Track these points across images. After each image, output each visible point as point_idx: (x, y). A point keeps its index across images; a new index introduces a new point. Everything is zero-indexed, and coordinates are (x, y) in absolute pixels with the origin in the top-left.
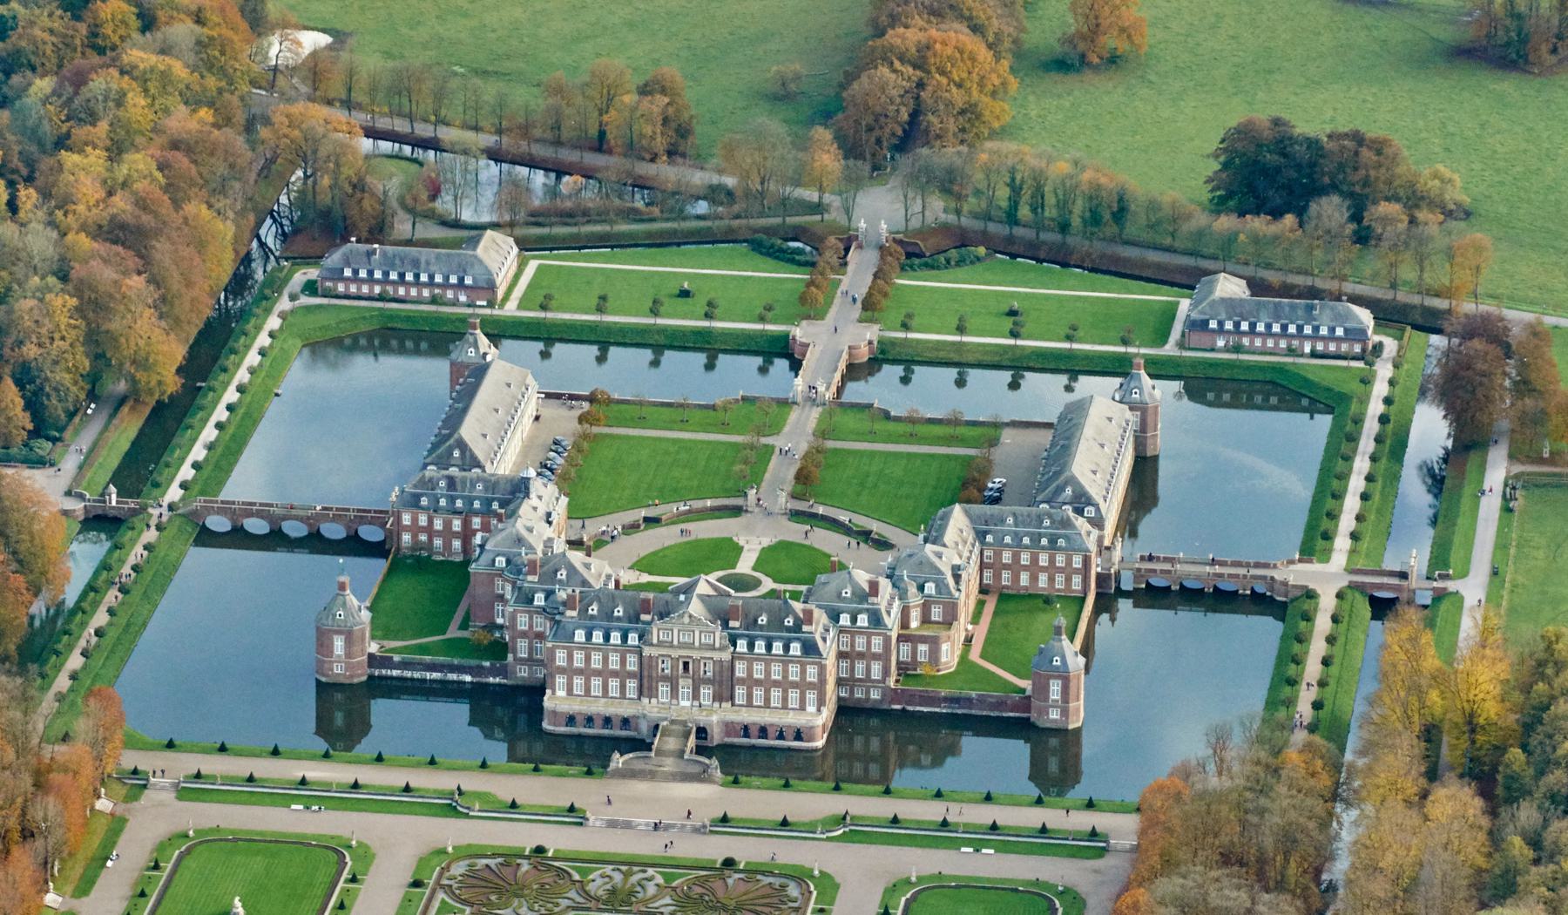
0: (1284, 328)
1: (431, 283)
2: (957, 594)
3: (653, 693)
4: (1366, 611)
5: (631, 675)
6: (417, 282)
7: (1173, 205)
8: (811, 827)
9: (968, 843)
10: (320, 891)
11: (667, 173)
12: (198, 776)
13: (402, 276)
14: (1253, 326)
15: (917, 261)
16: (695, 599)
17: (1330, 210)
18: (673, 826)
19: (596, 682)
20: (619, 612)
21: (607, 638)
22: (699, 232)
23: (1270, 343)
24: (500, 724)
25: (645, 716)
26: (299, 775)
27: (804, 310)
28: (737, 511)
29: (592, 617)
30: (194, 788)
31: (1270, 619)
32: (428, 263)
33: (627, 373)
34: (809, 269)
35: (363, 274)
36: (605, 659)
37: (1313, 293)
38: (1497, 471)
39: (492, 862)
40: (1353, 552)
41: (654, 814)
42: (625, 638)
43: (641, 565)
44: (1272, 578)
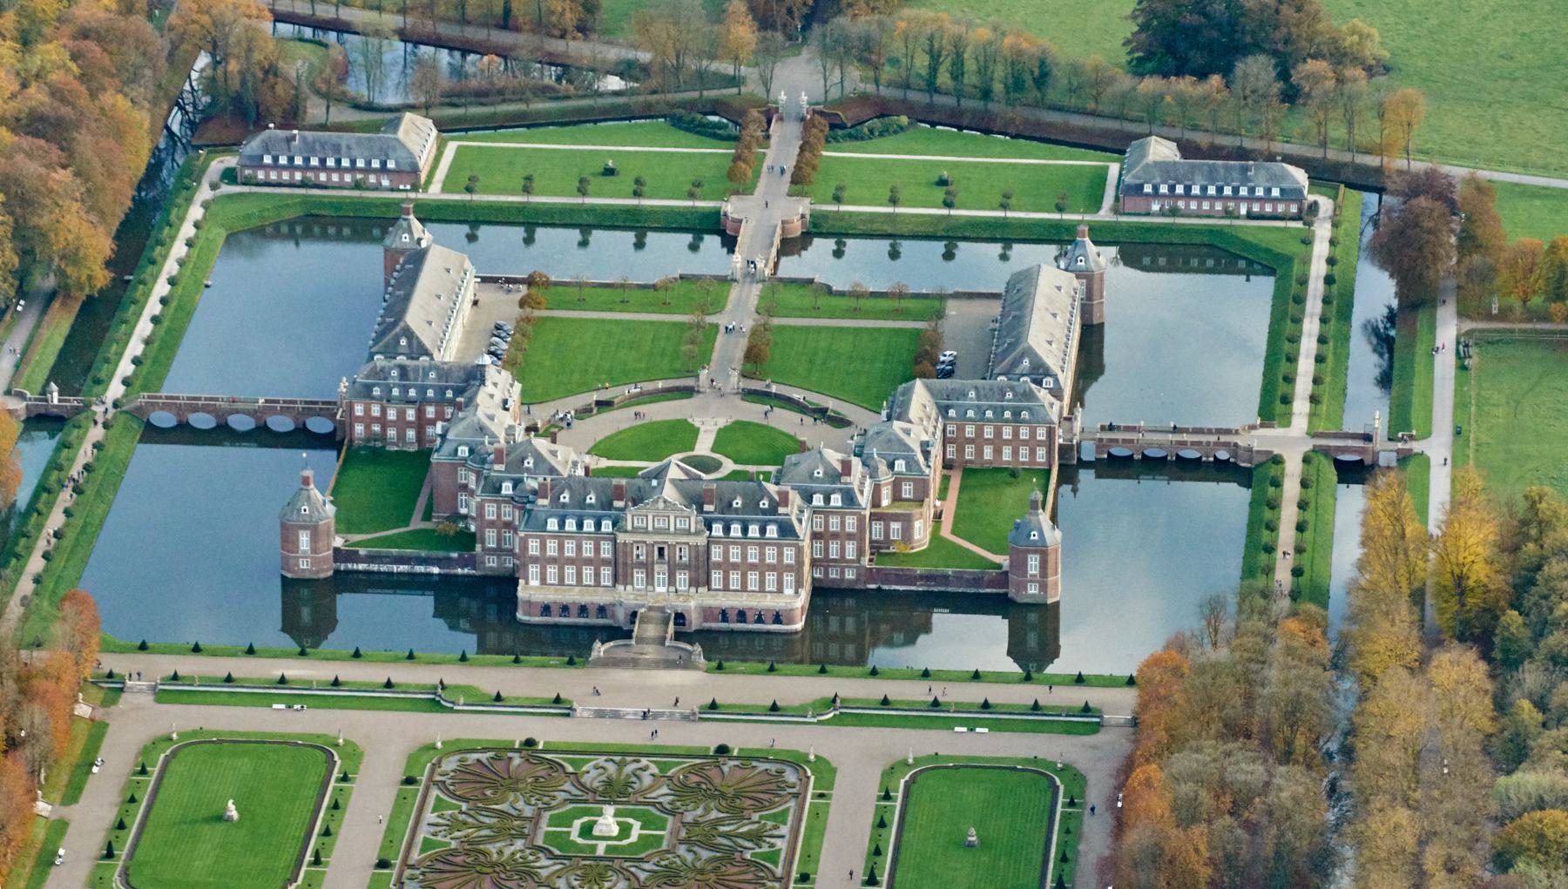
0: (1220, 190)
1: (353, 168)
2: (927, 471)
3: (628, 580)
4: (1331, 473)
5: (605, 562)
6: (338, 167)
7: (1096, 69)
8: (801, 711)
9: (962, 722)
10: (312, 792)
11: (578, 49)
12: (175, 677)
13: (323, 161)
14: (1188, 189)
15: (840, 132)
16: (668, 485)
17: (1257, 69)
18: (662, 714)
19: (570, 571)
20: (591, 499)
21: (580, 525)
22: (614, 108)
23: (1206, 206)
24: (466, 614)
25: (621, 604)
26: (277, 674)
27: (733, 186)
28: (688, 392)
29: (564, 505)
30: (172, 690)
31: (1234, 486)
32: (349, 147)
33: (557, 253)
34: (733, 143)
35: (283, 161)
36: (579, 548)
37: (1242, 154)
38: (1448, 329)
39: (484, 757)
40: (1312, 415)
41: (640, 703)
42: (598, 525)
43: (598, 450)
44: (1236, 445)
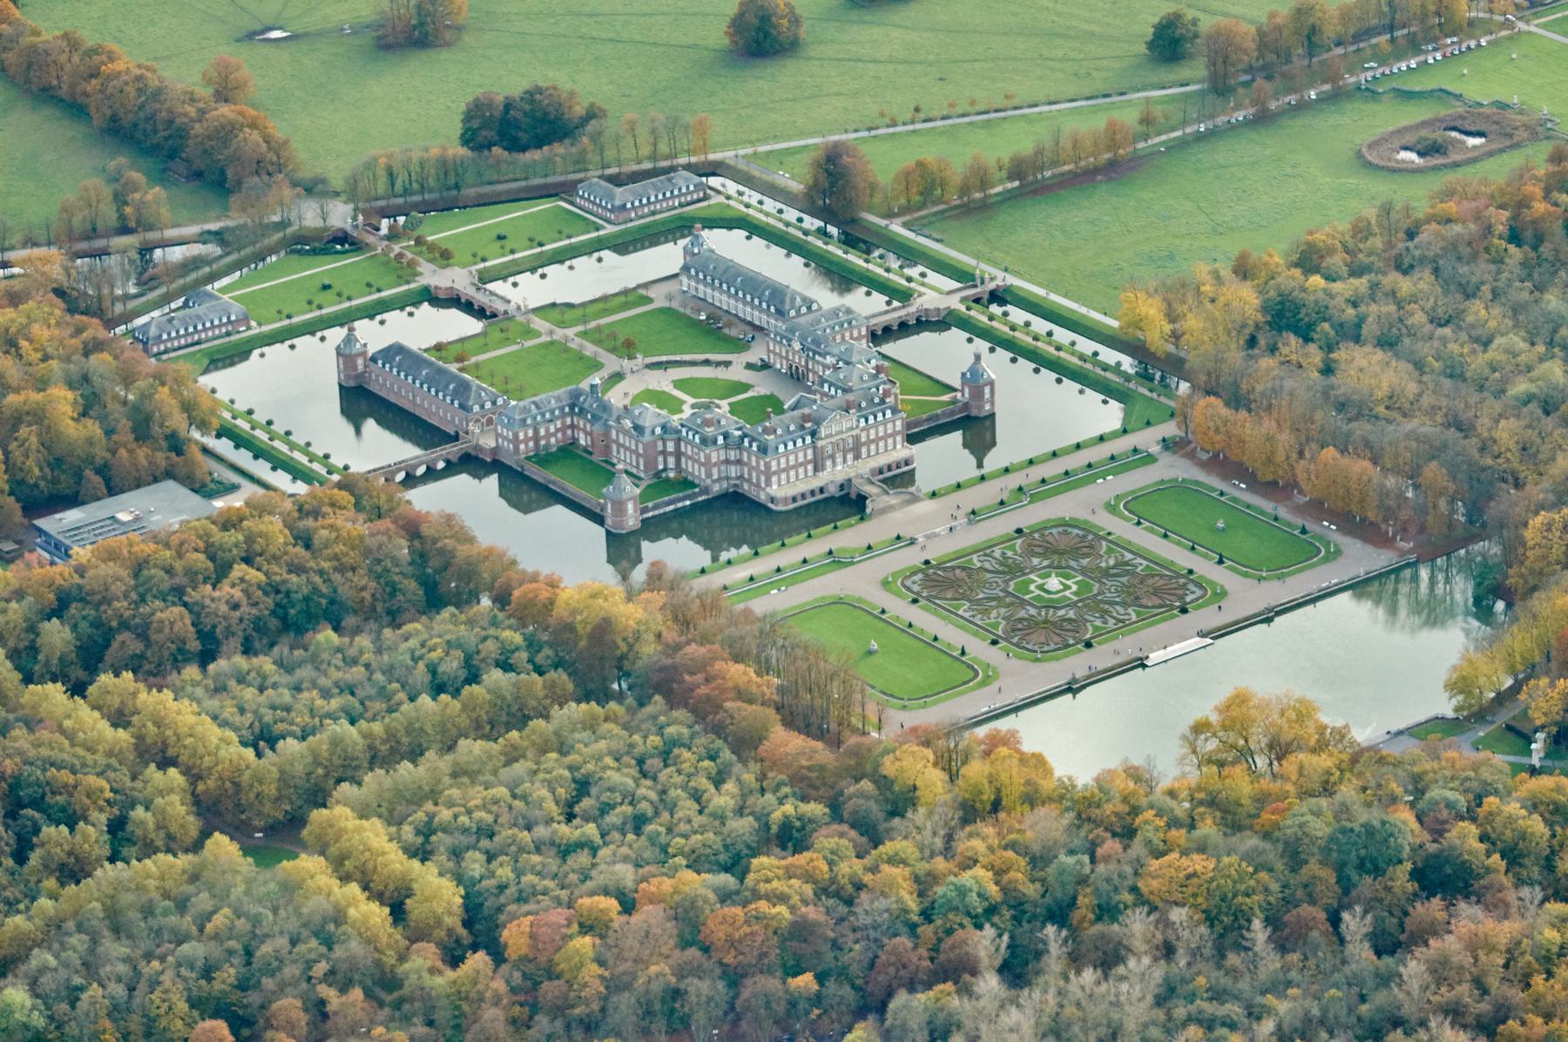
6: (205, 330)
20: (792, 428)
35: (173, 334)
39: (920, 576)
40: (923, 284)
